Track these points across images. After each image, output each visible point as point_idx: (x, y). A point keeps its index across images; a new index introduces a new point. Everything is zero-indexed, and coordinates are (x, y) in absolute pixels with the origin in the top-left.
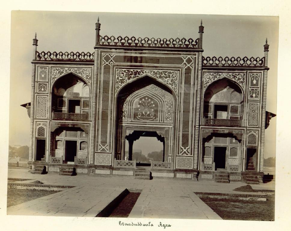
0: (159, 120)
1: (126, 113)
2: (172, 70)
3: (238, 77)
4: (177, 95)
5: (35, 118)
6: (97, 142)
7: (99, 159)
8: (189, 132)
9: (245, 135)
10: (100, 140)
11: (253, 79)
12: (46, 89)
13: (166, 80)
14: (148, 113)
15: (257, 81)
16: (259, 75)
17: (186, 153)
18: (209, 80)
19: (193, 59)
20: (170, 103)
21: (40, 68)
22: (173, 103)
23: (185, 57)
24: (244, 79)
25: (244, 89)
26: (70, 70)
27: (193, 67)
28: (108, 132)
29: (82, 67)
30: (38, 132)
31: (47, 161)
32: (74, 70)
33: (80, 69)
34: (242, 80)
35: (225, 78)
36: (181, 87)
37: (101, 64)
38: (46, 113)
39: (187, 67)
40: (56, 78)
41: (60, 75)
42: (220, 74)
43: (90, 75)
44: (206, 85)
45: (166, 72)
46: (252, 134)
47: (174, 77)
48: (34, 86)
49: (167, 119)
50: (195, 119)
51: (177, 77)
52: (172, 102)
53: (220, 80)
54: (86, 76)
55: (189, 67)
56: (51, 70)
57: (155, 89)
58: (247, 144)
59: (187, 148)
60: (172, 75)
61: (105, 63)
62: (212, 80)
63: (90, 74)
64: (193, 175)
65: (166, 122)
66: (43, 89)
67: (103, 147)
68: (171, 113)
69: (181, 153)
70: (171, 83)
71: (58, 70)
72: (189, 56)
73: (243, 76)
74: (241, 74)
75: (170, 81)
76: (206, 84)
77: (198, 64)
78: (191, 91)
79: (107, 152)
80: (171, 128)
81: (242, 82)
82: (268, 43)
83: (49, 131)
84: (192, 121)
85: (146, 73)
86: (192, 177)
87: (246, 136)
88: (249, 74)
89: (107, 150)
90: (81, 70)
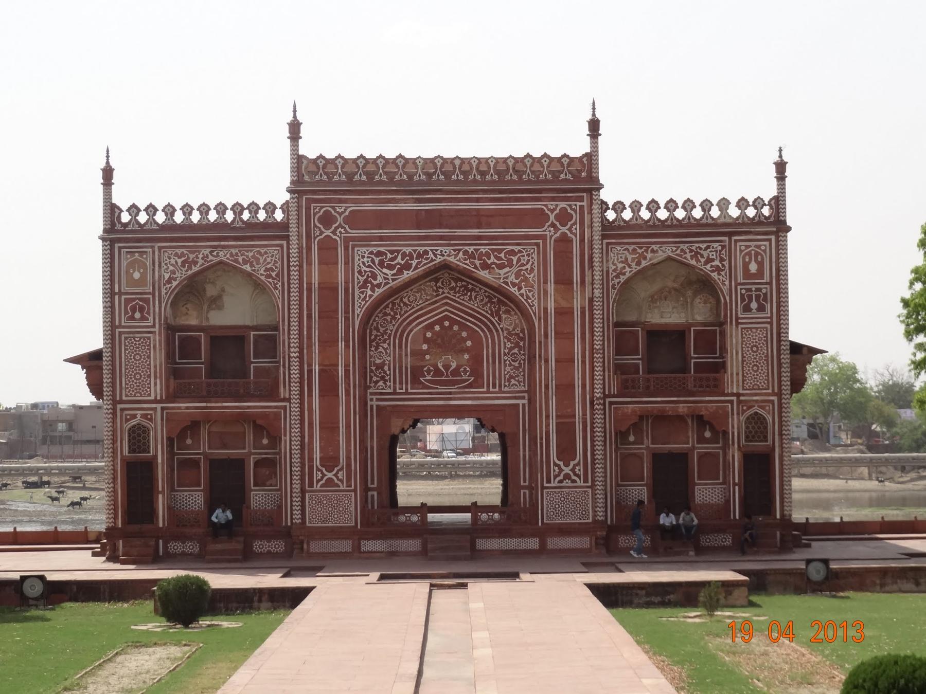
1: (389, 369)
3: (705, 254)
4: (535, 314)
5: (118, 399)
6: (311, 459)
8: (574, 416)
9: (735, 416)
10: (317, 455)
11: (747, 260)
12: (148, 313)
14: (454, 365)
15: (761, 265)
18: (624, 268)
19: (575, 211)
20: (517, 335)
22: (524, 335)
24: (722, 260)
25: (725, 289)
26: (218, 256)
27: (575, 235)
29: (253, 246)
30: (129, 441)
31: (161, 525)
32: (228, 256)
33: (247, 251)
35: (669, 259)
36: (546, 292)
38: (150, 384)
39: (558, 235)
40: (175, 279)
42: (655, 247)
44: (617, 281)
45: (500, 251)
46: (756, 413)
47: (523, 265)
48: (112, 307)
49: (509, 381)
52: (523, 331)
53: (653, 265)
55: (564, 234)
56: (159, 259)
57: (470, 296)
59: (572, 463)
60: (519, 260)
62: (633, 265)
64: (594, 539)
65: (506, 389)
66: (137, 315)
67: (330, 475)
69: (558, 479)
70: (517, 281)
71: (179, 258)
72: (562, 205)
73: (721, 251)
74: (716, 245)
75: (513, 276)
76: (617, 277)
77: (591, 227)
80: (524, 405)
81: (718, 270)
82: (785, 159)
84: (584, 386)
85: (443, 255)
87: (739, 419)
88: (736, 246)
90: (251, 254)
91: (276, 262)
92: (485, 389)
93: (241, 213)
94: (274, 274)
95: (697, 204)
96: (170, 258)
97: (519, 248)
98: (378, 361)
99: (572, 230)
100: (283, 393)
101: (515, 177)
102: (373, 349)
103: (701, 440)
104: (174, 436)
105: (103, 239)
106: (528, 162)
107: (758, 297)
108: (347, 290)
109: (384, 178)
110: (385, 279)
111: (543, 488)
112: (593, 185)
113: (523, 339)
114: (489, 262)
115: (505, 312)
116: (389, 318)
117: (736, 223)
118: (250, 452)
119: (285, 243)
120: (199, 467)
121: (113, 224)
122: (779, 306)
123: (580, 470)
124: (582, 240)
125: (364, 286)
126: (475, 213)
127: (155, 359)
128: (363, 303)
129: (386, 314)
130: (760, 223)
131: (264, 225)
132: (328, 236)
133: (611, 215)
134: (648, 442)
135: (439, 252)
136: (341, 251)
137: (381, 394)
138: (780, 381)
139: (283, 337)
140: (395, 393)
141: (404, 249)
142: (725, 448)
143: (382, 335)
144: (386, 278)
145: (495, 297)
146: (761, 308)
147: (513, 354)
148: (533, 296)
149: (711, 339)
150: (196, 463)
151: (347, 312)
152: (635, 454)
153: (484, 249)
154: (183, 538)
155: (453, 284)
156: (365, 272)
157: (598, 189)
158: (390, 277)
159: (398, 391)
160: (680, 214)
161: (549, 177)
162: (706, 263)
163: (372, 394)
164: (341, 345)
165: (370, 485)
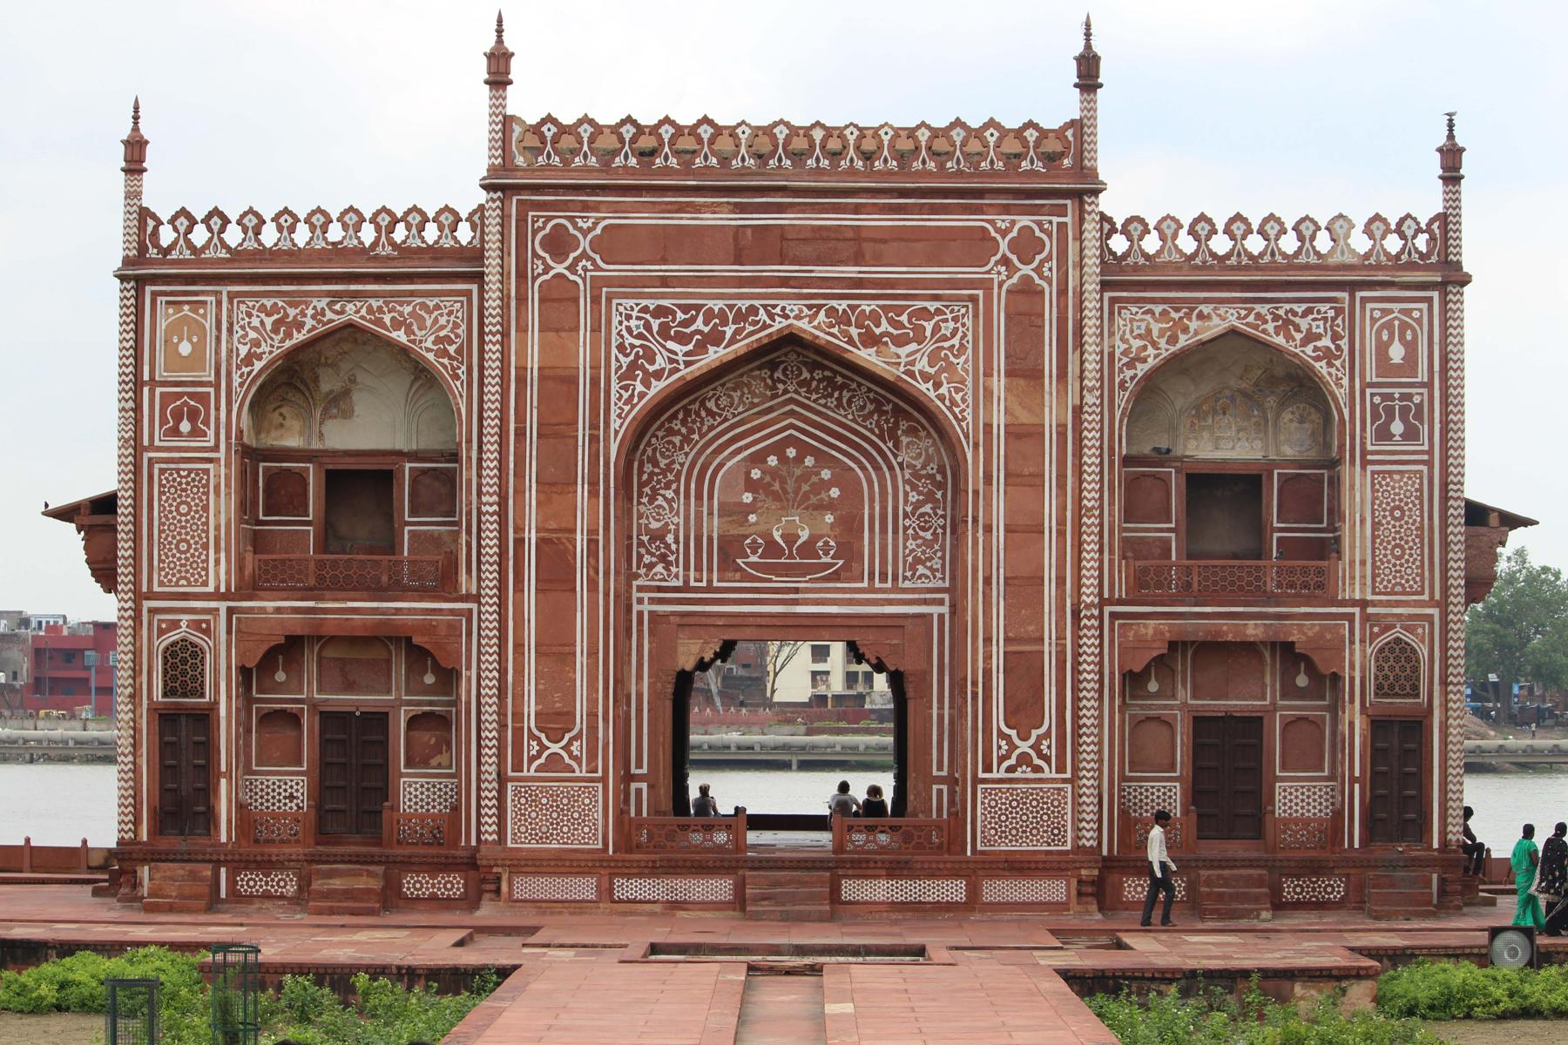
0: (872, 574)
1: (677, 541)
2: (936, 298)
3: (1304, 324)
4: (967, 436)
5: (145, 589)
6: (518, 716)
7: (533, 815)
8: (1042, 639)
9: (1357, 646)
10: (531, 708)
11: (1385, 338)
12: (206, 423)
13: (899, 357)
14: (804, 535)
15: (1411, 348)
16: (1416, 314)
17: (1029, 763)
18: (1145, 348)
19: (1050, 236)
20: (931, 477)
21: (168, 303)
22: (945, 477)
23: (1006, 226)
24: (1336, 337)
25: (1341, 394)
26: (342, 312)
28: (581, 660)
29: (412, 294)
30: (165, 672)
31: (224, 839)
34: (1326, 342)
35: (1233, 332)
36: (988, 393)
37: (521, 275)
38: (207, 561)
39: (1015, 280)
41: (282, 341)
42: (1206, 309)
43: (457, 336)
44: (1130, 373)
45: (900, 310)
46: (1398, 641)
47: (945, 338)
48: (137, 409)
49: (913, 568)
50: (1078, 568)
51: (965, 335)
53: (1203, 344)
54: (434, 343)
55: (1026, 279)
56: (230, 317)
57: (839, 399)
58: (1370, 696)
59: (1035, 733)
60: (936, 329)
61: (547, 269)
62: (1162, 343)
63: (459, 331)
64: (1074, 882)
65: (907, 584)
66: (185, 426)
67: (555, 748)
68: (940, 531)
69: (1006, 764)
70: (932, 371)
71: (269, 315)
72: (1024, 221)
73: (1334, 319)
74: (1324, 307)
75: (925, 359)
76: (1130, 365)
77: (1081, 266)
78: (1047, 410)
79: (577, 774)
80: (941, 616)
81: (1328, 356)
82: (1460, 141)
83: (229, 668)
85: (786, 317)
86: (1068, 896)
87: (1363, 651)
89: (578, 760)
90: (407, 309)
91: (456, 326)
92: (865, 584)
93: (391, 229)
94: (452, 349)
95: (1289, 225)
96: (249, 315)
97: (937, 304)
98: (655, 525)
99: (1042, 272)
100: (466, 584)
101: (931, 165)
102: (645, 500)
103: (1289, 691)
104: (251, 664)
105: (123, 278)
106: (958, 135)
107: (1405, 412)
108: (595, 382)
109: (673, 162)
110: (671, 361)
111: (976, 781)
112: (1086, 188)
113: (941, 486)
114: (878, 331)
115: (907, 432)
116: (677, 440)
117: (1364, 263)
118: (398, 698)
119: (474, 288)
120: (299, 725)
121: (142, 249)
122: (1445, 430)
123: (1050, 747)
124: (1062, 292)
125: (629, 374)
126: (850, 235)
127: (218, 512)
128: (627, 408)
129: (671, 432)
130: (1411, 266)
131: (435, 252)
132: (559, 276)
133: (1119, 244)
134: (1184, 694)
135: (778, 310)
136: (584, 305)
137: (660, 589)
138: (1445, 578)
139: (468, 474)
140: (686, 588)
141: (710, 303)
142: (1335, 709)
143: (663, 473)
144: (676, 362)
145: (889, 401)
146: (1411, 434)
147: (923, 515)
148: (964, 400)
149: (1314, 493)
150: (294, 719)
151: (594, 426)
152: (1158, 719)
153: (867, 306)
154: (266, 866)
155: (806, 375)
156: (633, 346)
157: (1096, 193)
158: (681, 358)
159: (693, 583)
160: (1255, 244)
161: (999, 165)
162: (1306, 341)
163: (640, 589)
164: (582, 491)
165: (634, 770)
